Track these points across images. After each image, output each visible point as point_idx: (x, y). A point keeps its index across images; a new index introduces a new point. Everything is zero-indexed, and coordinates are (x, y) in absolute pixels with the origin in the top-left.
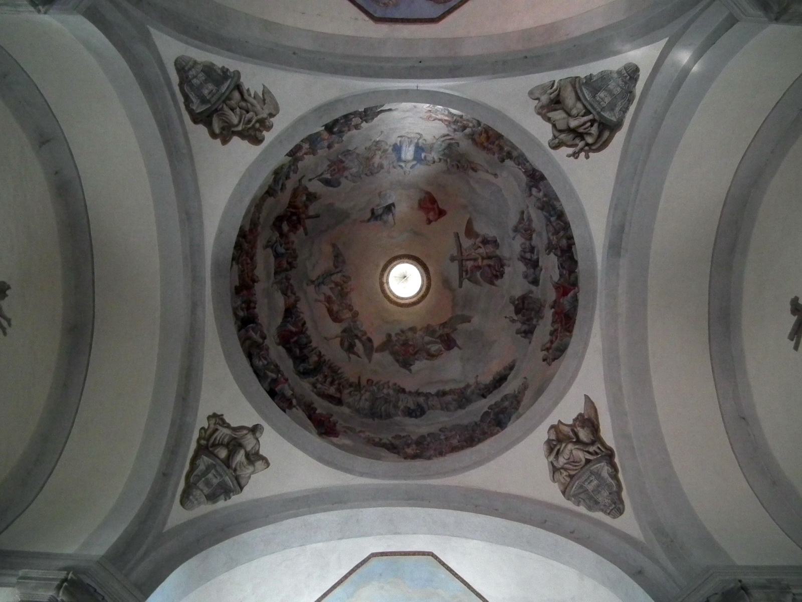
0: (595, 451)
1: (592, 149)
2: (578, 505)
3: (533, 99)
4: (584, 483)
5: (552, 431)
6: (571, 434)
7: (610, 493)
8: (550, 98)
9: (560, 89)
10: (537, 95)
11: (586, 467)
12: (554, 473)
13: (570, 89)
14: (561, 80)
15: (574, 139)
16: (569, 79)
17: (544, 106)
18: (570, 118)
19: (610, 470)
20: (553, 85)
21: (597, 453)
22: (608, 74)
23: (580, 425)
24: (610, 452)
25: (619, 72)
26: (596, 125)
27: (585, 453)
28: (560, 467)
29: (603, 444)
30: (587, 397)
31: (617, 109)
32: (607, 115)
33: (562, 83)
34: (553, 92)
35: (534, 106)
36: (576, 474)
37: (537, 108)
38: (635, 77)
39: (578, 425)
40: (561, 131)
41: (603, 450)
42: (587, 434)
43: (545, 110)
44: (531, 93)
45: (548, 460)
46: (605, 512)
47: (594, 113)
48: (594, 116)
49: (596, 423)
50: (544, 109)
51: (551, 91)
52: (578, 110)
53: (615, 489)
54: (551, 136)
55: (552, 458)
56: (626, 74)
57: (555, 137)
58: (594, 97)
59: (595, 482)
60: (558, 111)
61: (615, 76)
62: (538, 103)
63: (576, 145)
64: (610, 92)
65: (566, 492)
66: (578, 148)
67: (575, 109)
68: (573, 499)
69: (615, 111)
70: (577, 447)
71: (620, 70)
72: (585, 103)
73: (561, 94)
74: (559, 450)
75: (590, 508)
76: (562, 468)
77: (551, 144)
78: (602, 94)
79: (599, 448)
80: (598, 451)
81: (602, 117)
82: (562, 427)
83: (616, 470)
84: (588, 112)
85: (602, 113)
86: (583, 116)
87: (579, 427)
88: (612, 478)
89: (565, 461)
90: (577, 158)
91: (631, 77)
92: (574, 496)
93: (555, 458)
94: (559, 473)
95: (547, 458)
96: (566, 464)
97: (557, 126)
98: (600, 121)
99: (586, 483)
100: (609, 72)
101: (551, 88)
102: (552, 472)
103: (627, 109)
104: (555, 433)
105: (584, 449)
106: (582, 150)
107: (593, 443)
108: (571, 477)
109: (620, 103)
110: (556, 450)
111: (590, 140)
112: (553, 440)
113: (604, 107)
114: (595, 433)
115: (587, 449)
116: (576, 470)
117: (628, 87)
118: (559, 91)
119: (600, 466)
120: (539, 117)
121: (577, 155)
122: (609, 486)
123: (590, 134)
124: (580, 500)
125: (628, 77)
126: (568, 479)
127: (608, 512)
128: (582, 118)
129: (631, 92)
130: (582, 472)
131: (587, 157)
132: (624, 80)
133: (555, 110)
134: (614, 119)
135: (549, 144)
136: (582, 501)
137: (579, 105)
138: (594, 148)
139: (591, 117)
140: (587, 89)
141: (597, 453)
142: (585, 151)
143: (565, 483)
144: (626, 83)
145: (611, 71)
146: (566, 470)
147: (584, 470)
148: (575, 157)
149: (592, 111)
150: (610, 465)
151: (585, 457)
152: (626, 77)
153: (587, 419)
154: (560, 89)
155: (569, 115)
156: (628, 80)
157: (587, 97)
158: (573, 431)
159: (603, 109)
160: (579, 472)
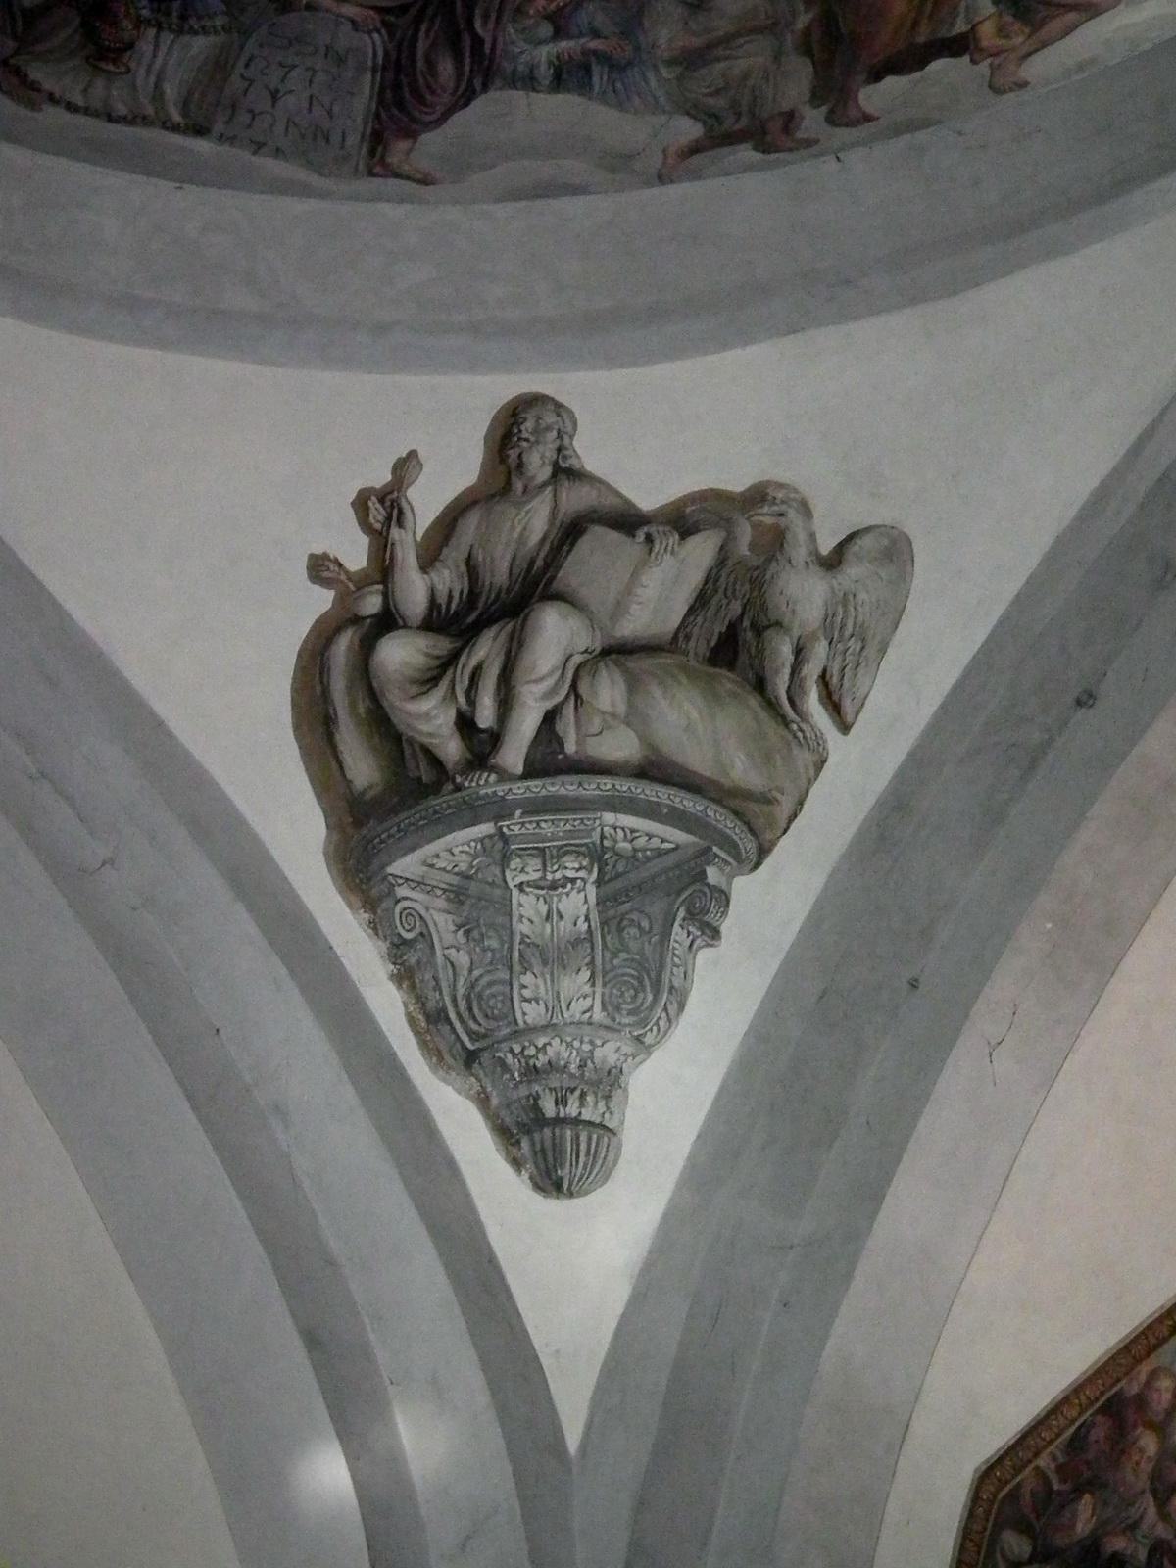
1: (338, 630)
3: (851, 538)
8: (787, 631)
9: (785, 722)
10: (853, 571)
13: (741, 771)
14: (820, 764)
15: (471, 567)
16: (786, 805)
17: (771, 559)
18: (598, 646)
20: (833, 703)
22: (643, 1023)
25: (609, 1083)
26: (452, 749)
31: (442, 923)
32: (457, 847)
33: (804, 757)
34: (795, 670)
35: (818, 513)
37: (794, 517)
38: (525, 1144)
40: (571, 532)
43: (745, 534)
44: (896, 551)
47: (519, 790)
48: (504, 776)
50: (753, 546)
51: (811, 671)
52: (596, 724)
54: (591, 453)
56: (572, 1109)
57: (565, 472)
58: (597, 855)
60: (680, 608)
61: (608, 1053)
62: (812, 536)
63: (430, 558)
64: (553, 957)
66: (407, 558)
67: (622, 708)
69: (441, 903)
71: (617, 1094)
72: (607, 783)
73: (754, 701)
77: (550, 418)
78: (577, 905)
81: (473, 812)
84: (548, 758)
85: (486, 829)
86: (550, 718)
90: (361, 504)
91: (540, 1121)
97: (614, 536)
98: (458, 788)
100: (648, 1039)
101: (824, 679)
103: (405, 976)
106: (383, 568)
109: (462, 959)
111: (400, 654)
113: (504, 860)
117: (502, 1063)
118: (772, 705)
120: (737, 482)
121: (377, 514)
123: (429, 680)
125: (549, 1108)
128: (549, 704)
129: (470, 1059)
131: (320, 568)
132: (555, 1081)
133: (701, 601)
134: (407, 865)
135: (559, 407)
137: (620, 746)
138: (344, 644)
139: (513, 754)
140: (660, 853)
142: (362, 581)
144: (532, 1072)
145: (648, 1050)
148: (374, 504)
149: (538, 787)
152: (561, 1102)
154: (785, 722)
155: (617, 652)
156: (537, 1097)
157: (629, 821)
159: (501, 850)
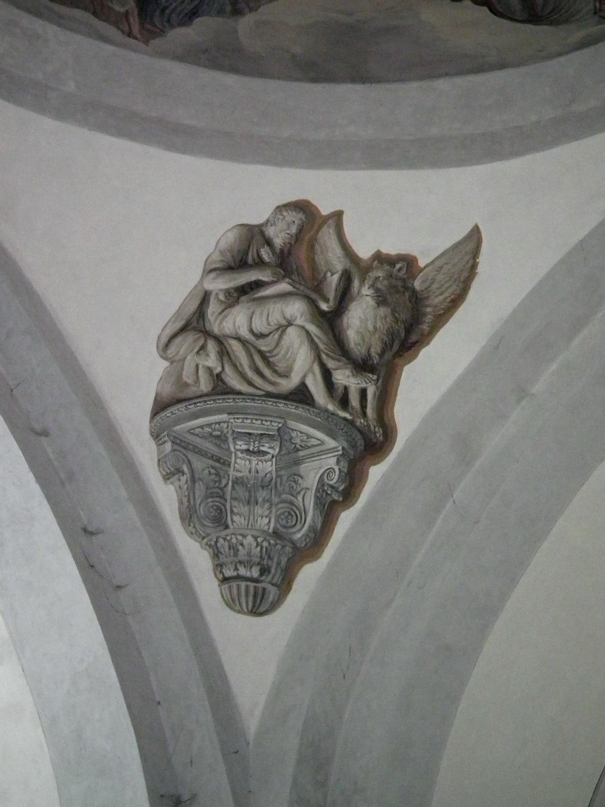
0: (346, 388)
2: (167, 477)
4: (238, 436)
5: (295, 218)
6: (333, 280)
7: (276, 534)
11: (281, 405)
12: (183, 330)
19: (334, 479)
21: (344, 402)
23: (379, 285)
24: (379, 432)
27: (317, 369)
28: (216, 330)
29: (386, 397)
30: (475, 237)
36: (239, 393)
39: (377, 278)
41: (370, 411)
42: (371, 327)
45: (202, 278)
46: (219, 566)
49: (425, 327)
53: (299, 534)
55: (219, 285)
59: (267, 467)
65: (167, 413)
68: (168, 446)
70: (312, 328)
74: (258, 285)
75: (188, 516)
76: (219, 341)
79: (363, 393)
80: (355, 401)
82: (328, 237)
83: (349, 494)
87: (372, 286)
88: (319, 501)
89: (244, 333)
92: (180, 443)
93: (228, 292)
94: (201, 342)
95: (209, 271)
96: (239, 339)
99: (242, 445)
102: (179, 325)
104: (294, 230)
105: (324, 356)
107: (362, 366)
108: (220, 388)
110: (252, 276)
112: (269, 242)
114: (396, 347)
115: (330, 364)
116: (251, 384)
119: (322, 443)
122: (293, 514)
124: (185, 468)
126: (205, 385)
127: (229, 573)
130: (257, 404)
136: (188, 476)
141: (344, 402)
143: (186, 385)
146: (224, 353)
147: (270, 404)
150: (344, 465)
151: (305, 376)
153: (414, 291)
158: (347, 278)
160: (252, 397)
